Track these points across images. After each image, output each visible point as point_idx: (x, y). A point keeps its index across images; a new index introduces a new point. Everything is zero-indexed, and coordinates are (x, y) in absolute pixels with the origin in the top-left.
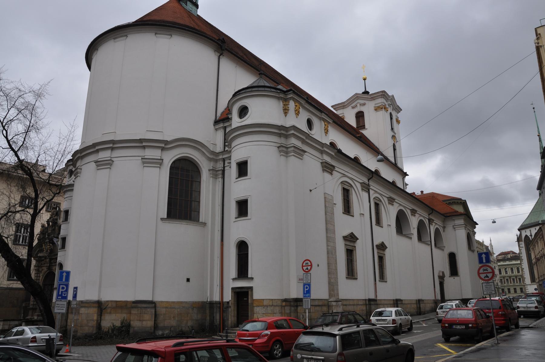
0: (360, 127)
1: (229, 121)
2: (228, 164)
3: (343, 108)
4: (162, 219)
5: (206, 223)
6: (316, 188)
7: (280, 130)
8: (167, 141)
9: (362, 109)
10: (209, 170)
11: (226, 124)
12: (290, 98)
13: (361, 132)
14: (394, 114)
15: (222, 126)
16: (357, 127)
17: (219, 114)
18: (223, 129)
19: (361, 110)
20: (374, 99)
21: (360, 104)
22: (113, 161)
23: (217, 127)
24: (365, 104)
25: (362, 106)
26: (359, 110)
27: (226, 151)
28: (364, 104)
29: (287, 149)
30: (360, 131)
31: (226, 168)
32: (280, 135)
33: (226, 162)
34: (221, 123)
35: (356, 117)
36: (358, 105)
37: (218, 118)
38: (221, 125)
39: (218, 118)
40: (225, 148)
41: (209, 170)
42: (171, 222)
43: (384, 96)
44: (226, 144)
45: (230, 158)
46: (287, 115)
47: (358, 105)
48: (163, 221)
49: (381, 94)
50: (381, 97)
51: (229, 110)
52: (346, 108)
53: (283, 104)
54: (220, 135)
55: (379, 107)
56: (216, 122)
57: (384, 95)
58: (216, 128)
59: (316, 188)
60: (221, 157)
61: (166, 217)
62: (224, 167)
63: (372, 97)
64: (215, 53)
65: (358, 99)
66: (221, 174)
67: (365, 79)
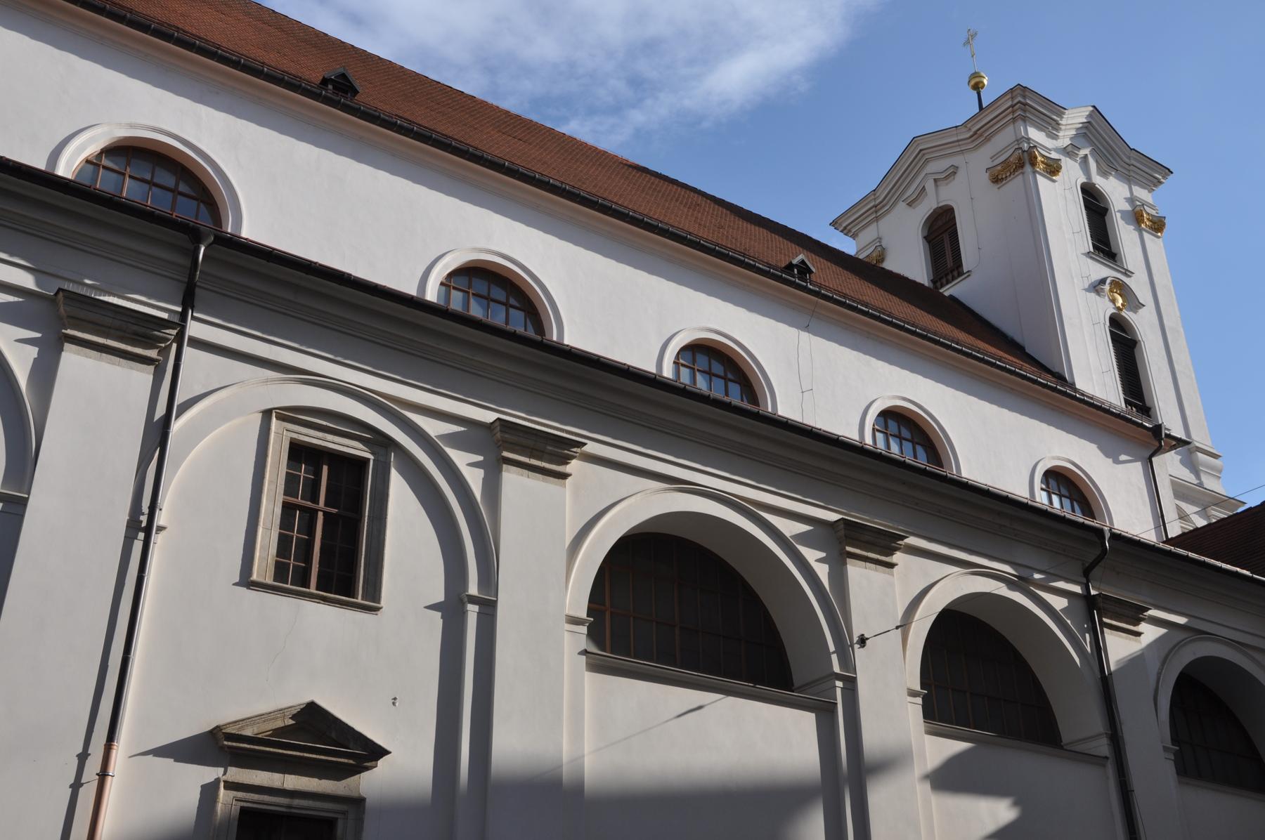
3: (877, 219)
9: (950, 195)
13: (947, 294)
14: (1116, 192)
16: (934, 282)
19: (941, 205)
20: (988, 139)
24: (954, 173)
26: (935, 206)
28: (953, 172)
30: (942, 294)
35: (925, 238)
36: (930, 185)
43: (1025, 111)
47: (930, 185)
49: (1010, 103)
50: (1011, 117)
52: (888, 211)
63: (975, 133)
65: (927, 161)
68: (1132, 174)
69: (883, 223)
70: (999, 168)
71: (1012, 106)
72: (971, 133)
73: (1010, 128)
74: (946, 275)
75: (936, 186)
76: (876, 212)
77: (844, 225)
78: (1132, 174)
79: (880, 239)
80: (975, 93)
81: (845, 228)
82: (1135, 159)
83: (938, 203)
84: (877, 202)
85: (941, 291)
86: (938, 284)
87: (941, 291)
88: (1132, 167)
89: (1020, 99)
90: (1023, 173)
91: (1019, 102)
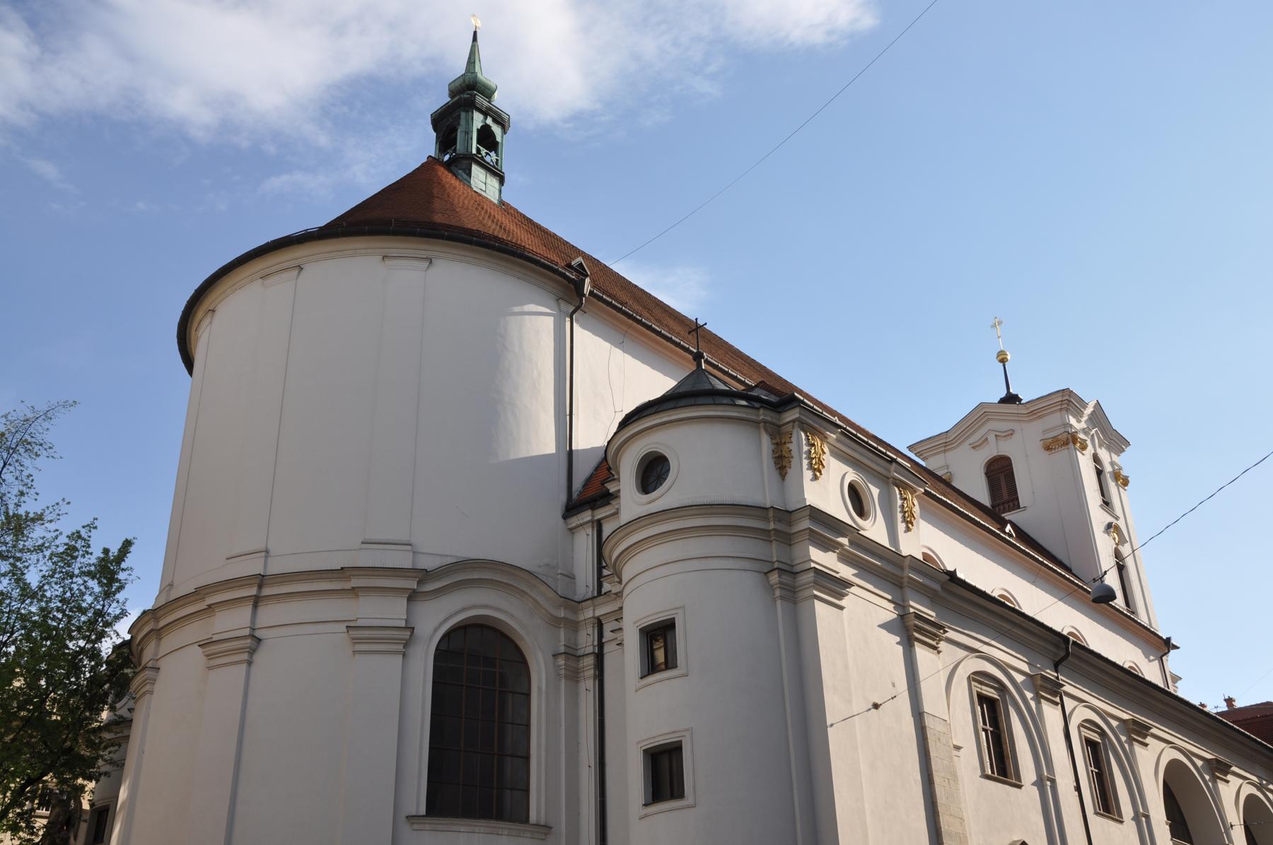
0: (1003, 503)
1: (608, 503)
2: (613, 635)
3: (945, 451)
4: (411, 818)
5: (551, 828)
6: (893, 698)
7: (767, 519)
8: (426, 570)
9: (1005, 448)
10: (553, 656)
11: (601, 513)
12: (794, 421)
15: (589, 518)
17: (578, 484)
18: (593, 527)
19: (1000, 454)
20: (1039, 417)
21: (996, 436)
22: (260, 640)
23: (574, 521)
25: (1004, 439)
27: (605, 593)
28: (1011, 433)
29: (794, 578)
31: (607, 649)
32: (765, 535)
33: (607, 628)
34: (586, 510)
35: (986, 474)
36: (992, 438)
37: (575, 496)
38: (586, 516)
39: (575, 496)
40: (600, 585)
41: (553, 656)
42: (439, 827)
43: (1068, 405)
44: (605, 572)
45: (618, 615)
46: (786, 473)
47: (992, 438)
48: (416, 827)
49: (1060, 399)
50: (1059, 407)
51: (609, 469)
52: (954, 448)
53: (774, 441)
54: (584, 544)
55: (1055, 439)
56: (571, 509)
57: (1070, 401)
58: (570, 527)
59: (893, 698)
60: (589, 613)
61: (423, 811)
62: (601, 645)
64: (559, 305)
66: (593, 666)
67: (1003, 361)
68: (1112, 445)
69: (949, 454)
70: (1050, 440)
71: (1062, 401)
72: (1028, 411)
73: (1058, 415)
74: (1003, 503)
75: (996, 439)
76: (945, 446)
77: (919, 450)
78: (1112, 445)
79: (948, 466)
80: (1002, 364)
81: (919, 452)
82: (1115, 437)
83: (998, 452)
84: (948, 440)
85: (1003, 515)
86: (997, 509)
87: (1003, 515)
88: (1112, 441)
89: (1067, 397)
90: (1068, 449)
91: (1067, 400)
